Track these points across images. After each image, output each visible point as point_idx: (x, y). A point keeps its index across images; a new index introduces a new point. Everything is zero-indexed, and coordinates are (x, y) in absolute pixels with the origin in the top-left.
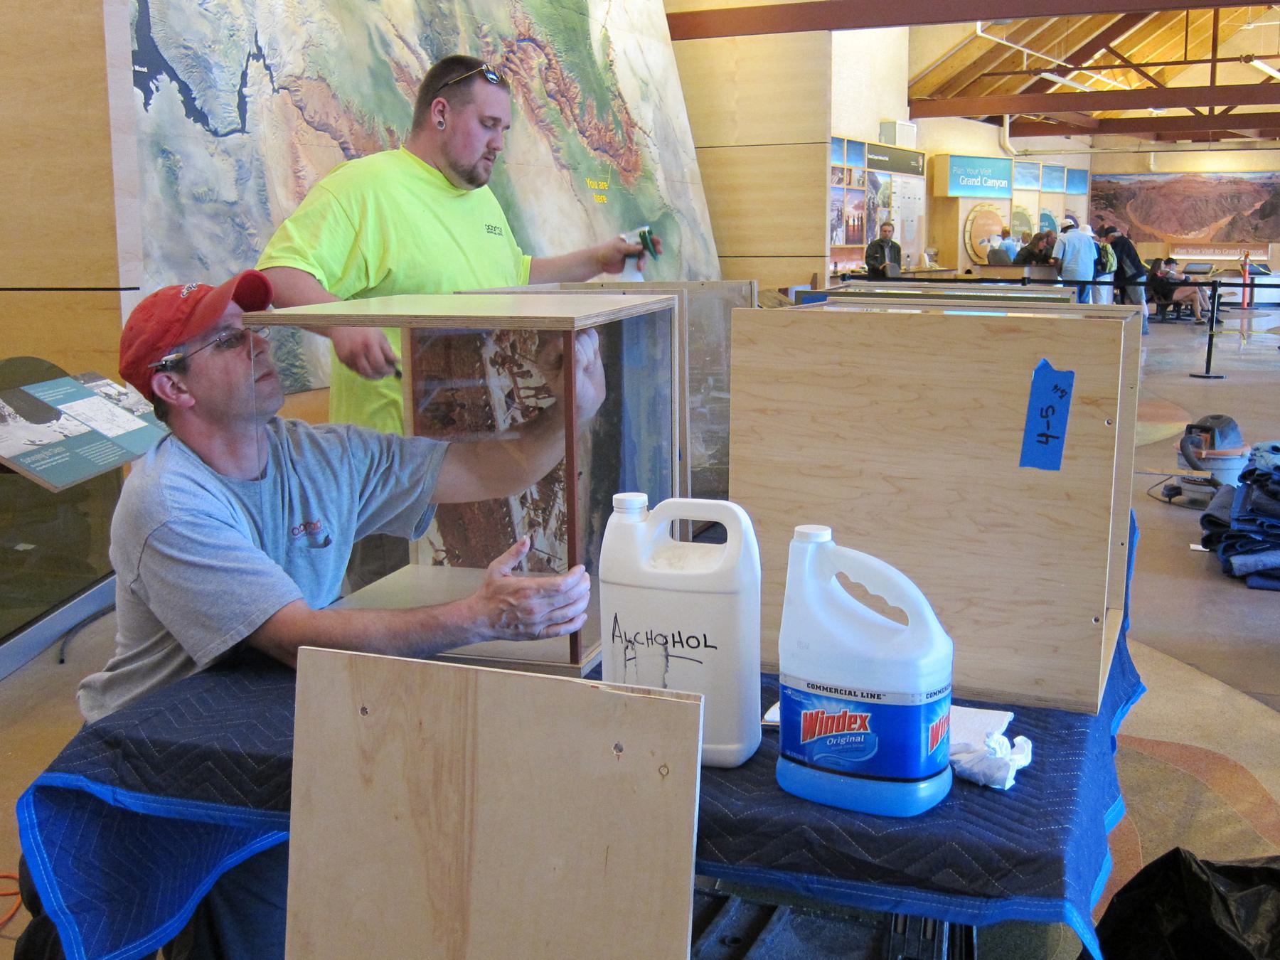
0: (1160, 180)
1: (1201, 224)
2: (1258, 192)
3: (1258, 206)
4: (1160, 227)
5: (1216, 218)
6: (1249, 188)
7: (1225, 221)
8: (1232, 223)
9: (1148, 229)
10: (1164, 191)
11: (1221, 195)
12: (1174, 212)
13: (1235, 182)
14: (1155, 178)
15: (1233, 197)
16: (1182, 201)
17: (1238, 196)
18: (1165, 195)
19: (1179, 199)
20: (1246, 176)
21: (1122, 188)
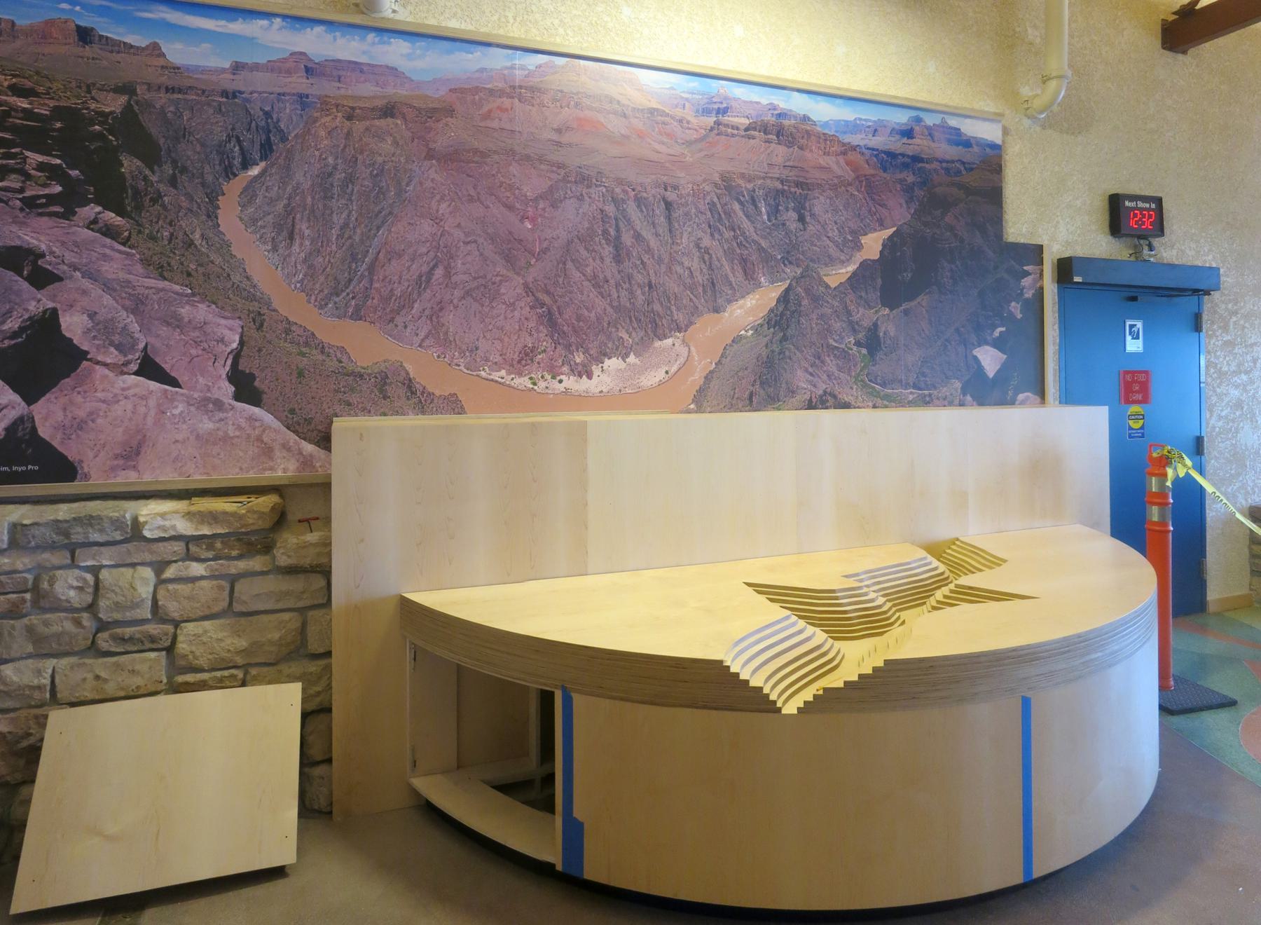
0: (423, 67)
1: (652, 321)
2: (870, 187)
3: (873, 244)
4: (440, 338)
5: (715, 295)
6: (837, 166)
7: (750, 308)
8: (781, 319)
9: (367, 346)
10: (447, 135)
11: (727, 184)
12: (512, 250)
13: (781, 130)
14: (395, 53)
15: (777, 197)
16: (551, 197)
17: (793, 193)
18: (452, 158)
19: (532, 185)
20: (823, 113)
21: (179, 84)
